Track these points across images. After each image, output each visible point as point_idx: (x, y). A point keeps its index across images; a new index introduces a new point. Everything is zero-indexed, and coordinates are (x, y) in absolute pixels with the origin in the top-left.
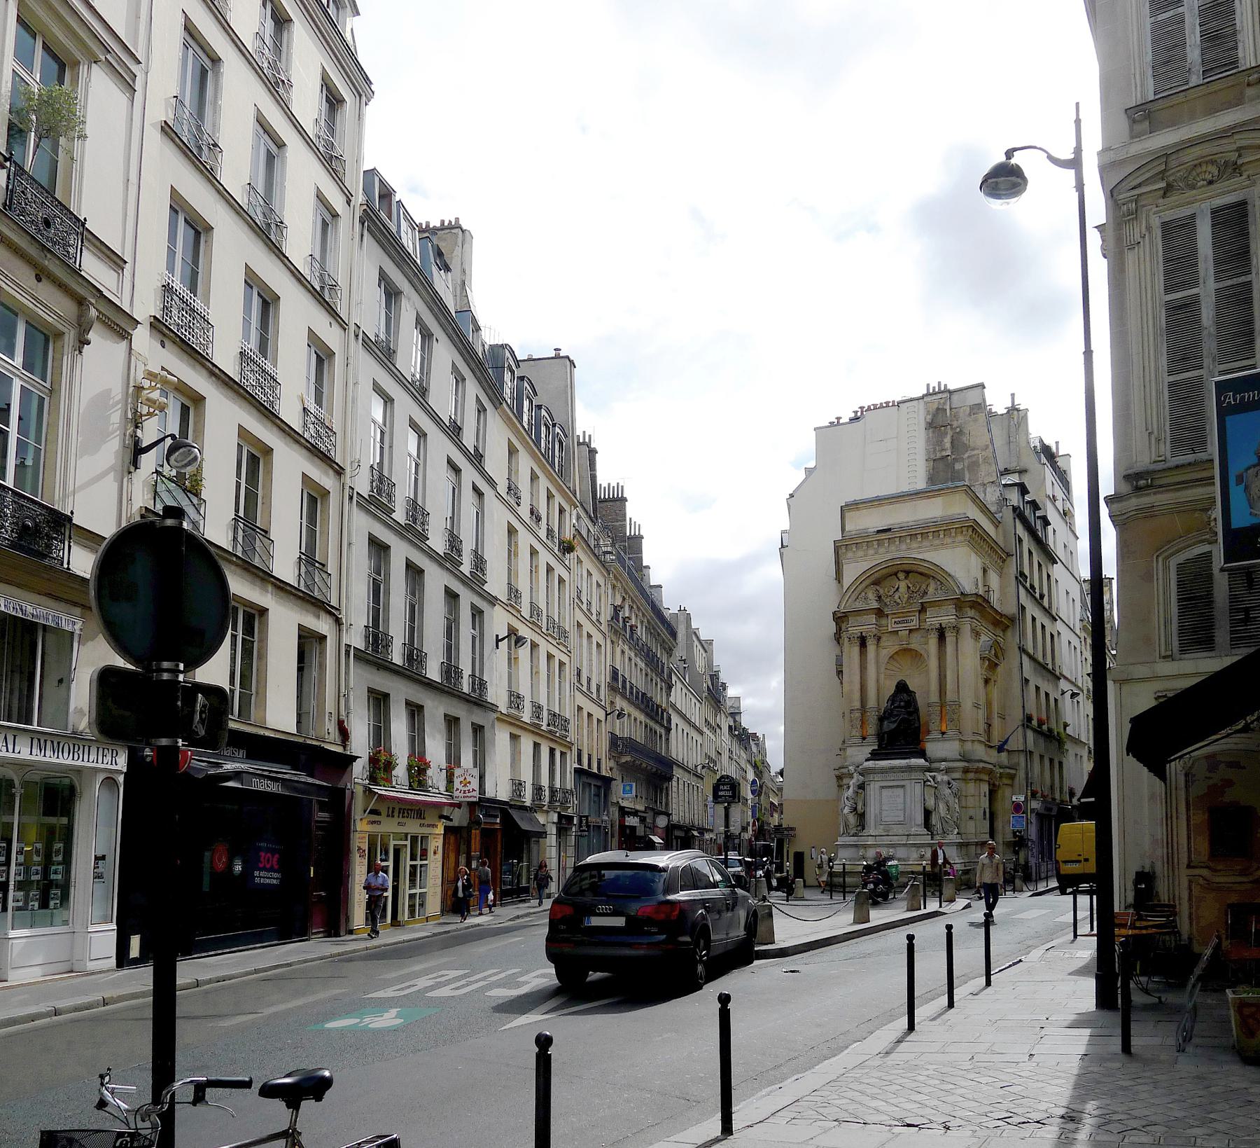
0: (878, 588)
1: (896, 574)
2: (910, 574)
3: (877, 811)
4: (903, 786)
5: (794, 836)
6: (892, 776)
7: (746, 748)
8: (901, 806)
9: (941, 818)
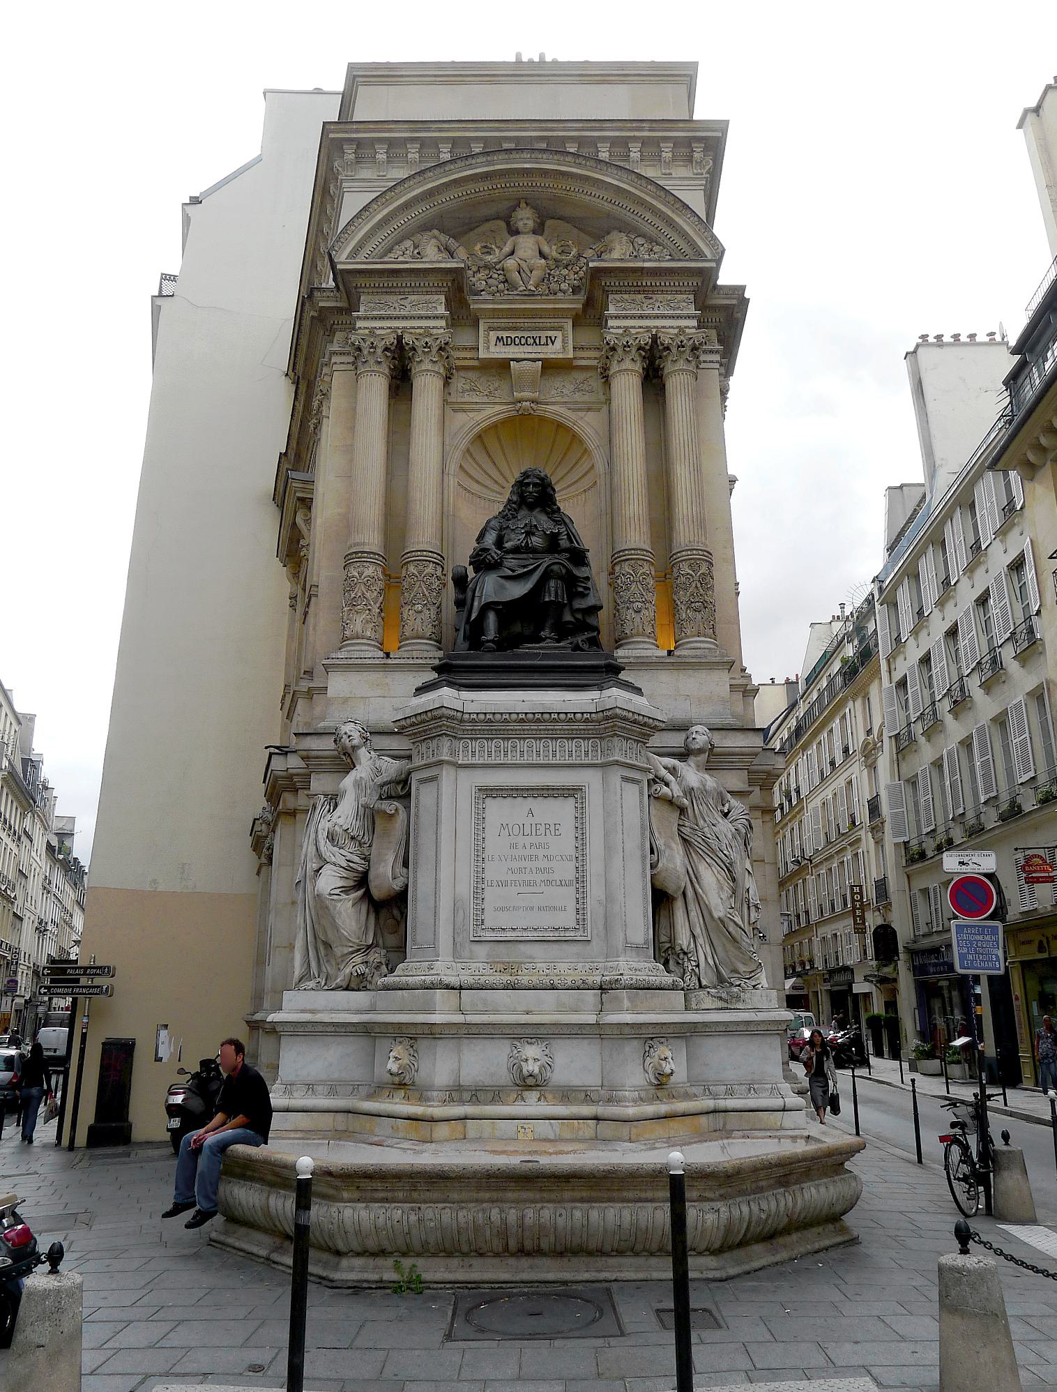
0: (452, 243)
3: (465, 889)
4: (571, 792)
5: (109, 992)
6: (529, 750)
7: (75, 884)
8: (567, 871)
9: (717, 928)
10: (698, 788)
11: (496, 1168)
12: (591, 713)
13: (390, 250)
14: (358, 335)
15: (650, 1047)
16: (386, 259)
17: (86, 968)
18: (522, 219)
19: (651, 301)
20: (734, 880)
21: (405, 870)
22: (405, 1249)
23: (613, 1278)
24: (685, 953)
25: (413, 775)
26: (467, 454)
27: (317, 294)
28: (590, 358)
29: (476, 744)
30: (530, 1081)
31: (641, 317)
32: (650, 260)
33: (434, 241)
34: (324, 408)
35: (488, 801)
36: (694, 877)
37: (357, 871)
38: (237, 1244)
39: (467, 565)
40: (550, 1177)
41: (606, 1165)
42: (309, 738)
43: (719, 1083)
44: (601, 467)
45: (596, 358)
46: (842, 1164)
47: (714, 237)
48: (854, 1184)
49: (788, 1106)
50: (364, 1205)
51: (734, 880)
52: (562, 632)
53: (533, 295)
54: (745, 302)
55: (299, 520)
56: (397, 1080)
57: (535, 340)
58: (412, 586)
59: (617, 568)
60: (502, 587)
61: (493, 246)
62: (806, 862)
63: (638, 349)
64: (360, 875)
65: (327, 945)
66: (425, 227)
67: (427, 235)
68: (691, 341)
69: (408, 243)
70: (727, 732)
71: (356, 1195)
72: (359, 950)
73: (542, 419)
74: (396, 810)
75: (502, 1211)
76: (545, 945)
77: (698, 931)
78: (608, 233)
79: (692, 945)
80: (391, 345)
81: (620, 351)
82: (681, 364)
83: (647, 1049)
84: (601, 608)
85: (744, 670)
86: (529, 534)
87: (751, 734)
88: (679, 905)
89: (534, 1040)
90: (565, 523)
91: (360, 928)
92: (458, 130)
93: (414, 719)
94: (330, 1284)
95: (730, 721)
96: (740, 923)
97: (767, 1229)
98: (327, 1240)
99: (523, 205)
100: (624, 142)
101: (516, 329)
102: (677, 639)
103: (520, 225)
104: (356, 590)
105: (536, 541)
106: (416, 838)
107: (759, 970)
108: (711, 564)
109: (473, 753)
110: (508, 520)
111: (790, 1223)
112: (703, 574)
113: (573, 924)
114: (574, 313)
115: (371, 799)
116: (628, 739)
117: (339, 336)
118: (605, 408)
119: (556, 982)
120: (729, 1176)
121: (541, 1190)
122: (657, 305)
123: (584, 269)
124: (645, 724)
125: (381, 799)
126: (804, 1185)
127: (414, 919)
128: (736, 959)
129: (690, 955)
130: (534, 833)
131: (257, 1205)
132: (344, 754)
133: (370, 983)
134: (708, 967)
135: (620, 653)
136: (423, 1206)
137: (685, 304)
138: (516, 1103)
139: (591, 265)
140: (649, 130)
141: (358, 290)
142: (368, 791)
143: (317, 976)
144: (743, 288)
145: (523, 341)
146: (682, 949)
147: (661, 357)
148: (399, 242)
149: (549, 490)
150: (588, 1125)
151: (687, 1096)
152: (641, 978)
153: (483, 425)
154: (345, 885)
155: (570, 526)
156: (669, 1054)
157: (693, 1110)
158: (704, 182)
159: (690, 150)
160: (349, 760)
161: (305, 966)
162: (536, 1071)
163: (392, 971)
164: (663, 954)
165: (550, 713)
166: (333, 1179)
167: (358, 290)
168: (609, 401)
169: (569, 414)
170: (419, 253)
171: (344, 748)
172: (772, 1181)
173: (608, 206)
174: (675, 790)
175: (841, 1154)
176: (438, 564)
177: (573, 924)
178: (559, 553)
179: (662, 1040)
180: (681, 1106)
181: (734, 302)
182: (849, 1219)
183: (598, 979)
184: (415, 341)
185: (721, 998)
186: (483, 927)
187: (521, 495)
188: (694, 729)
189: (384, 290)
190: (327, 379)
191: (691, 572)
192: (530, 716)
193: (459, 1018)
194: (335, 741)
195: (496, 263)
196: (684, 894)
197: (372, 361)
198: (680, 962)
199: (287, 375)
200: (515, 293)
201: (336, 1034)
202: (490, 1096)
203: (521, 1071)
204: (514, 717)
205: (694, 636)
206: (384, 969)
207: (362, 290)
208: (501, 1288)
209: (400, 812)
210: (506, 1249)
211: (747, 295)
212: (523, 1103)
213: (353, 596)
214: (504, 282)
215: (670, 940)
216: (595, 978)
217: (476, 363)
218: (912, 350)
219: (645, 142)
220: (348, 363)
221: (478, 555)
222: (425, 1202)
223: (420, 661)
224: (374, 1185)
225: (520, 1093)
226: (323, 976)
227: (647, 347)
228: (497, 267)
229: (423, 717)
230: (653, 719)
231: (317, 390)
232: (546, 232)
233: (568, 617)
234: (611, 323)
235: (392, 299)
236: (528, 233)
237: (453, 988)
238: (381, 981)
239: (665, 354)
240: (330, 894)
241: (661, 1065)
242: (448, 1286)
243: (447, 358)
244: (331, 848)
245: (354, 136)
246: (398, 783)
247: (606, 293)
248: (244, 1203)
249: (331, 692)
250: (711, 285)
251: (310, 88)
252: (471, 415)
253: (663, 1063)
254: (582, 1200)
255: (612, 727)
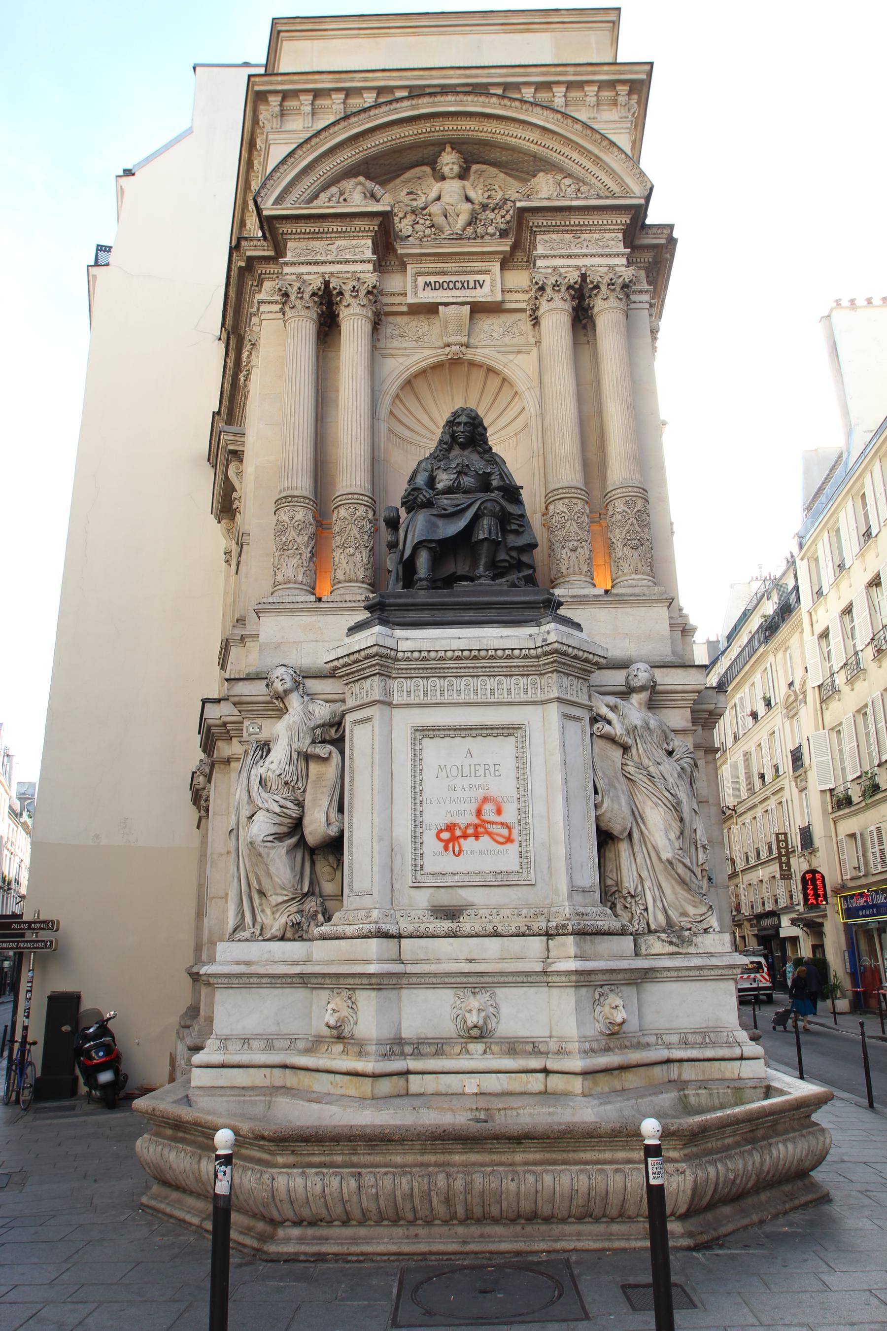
0: (377, 189)
1: (432, 163)
2: (475, 167)
10: (642, 726)
11: (441, 1130)
12: (529, 649)
13: (316, 197)
14: (285, 280)
15: (600, 995)
16: (311, 205)
17: (30, 923)
18: (448, 164)
19: (579, 240)
20: (681, 820)
21: (340, 816)
22: (345, 1218)
23: (572, 1247)
24: (632, 896)
25: (347, 716)
26: (398, 402)
27: (244, 243)
28: (519, 301)
29: (411, 683)
30: (475, 1032)
31: (570, 256)
32: (578, 198)
33: (359, 188)
34: (253, 357)
35: (426, 741)
36: (637, 816)
37: (291, 817)
38: (168, 1210)
39: (399, 506)
40: (501, 1139)
41: (560, 1124)
42: (241, 684)
43: (672, 1031)
44: (532, 407)
45: (524, 301)
46: (809, 1116)
47: (642, 174)
48: (822, 1139)
49: (746, 1054)
50: (300, 1170)
51: (681, 820)
52: (498, 570)
53: (460, 239)
54: (672, 242)
55: (231, 474)
56: (335, 1032)
57: (463, 284)
58: (343, 530)
59: (551, 507)
60: (435, 526)
61: (419, 192)
62: (731, 812)
63: (568, 288)
64: (294, 822)
65: (262, 893)
66: (350, 173)
67: (353, 181)
68: (621, 279)
69: (334, 190)
70: (669, 669)
71: (292, 1159)
72: (293, 899)
73: (472, 364)
74: (330, 754)
75: (448, 1175)
76: (487, 889)
77: (644, 874)
78: (535, 176)
79: (640, 888)
80: (319, 289)
81: (549, 290)
82: (612, 302)
83: (597, 996)
84: (536, 546)
85: (680, 610)
86: (459, 473)
87: (693, 671)
88: (624, 847)
89: (477, 990)
90: (496, 462)
91: (295, 876)
92: (384, 79)
93: (346, 659)
94: (265, 1257)
95: (670, 658)
96: (689, 864)
97: (734, 1190)
98: (262, 1209)
99: (448, 149)
100: (547, 86)
101: (443, 273)
102: (614, 576)
103: (446, 170)
104: (287, 534)
105: (468, 481)
106: (352, 780)
107: (710, 913)
108: (647, 501)
109: (409, 693)
110: (440, 461)
111: (757, 1182)
112: (639, 511)
113: (517, 868)
114: (501, 256)
115: (305, 744)
116: (569, 675)
117: (267, 285)
118: (535, 349)
119: (500, 929)
120: (694, 1135)
121: (490, 1152)
122: (585, 244)
123: (511, 212)
124: (586, 661)
125: (313, 742)
126: (773, 1140)
127: (351, 865)
128: (685, 901)
129: (637, 899)
130: (473, 774)
131: (188, 1169)
132: (277, 698)
133: (307, 932)
134: (657, 909)
135: (557, 592)
136: (363, 1171)
137: (613, 243)
138: (461, 1056)
139: (519, 205)
140: (574, 75)
141: (285, 237)
142: (301, 735)
143: (251, 926)
144: (671, 227)
145: (451, 285)
146: (629, 893)
147: (590, 297)
148: (324, 188)
149: (480, 429)
150: (537, 1079)
151: (639, 1046)
152: (589, 923)
153: (413, 370)
154: (278, 831)
155: (503, 467)
156: (619, 1002)
157: (648, 1061)
158: (629, 125)
159: (614, 93)
160: (282, 705)
161: (240, 916)
162: (481, 1022)
163: (328, 919)
164: (610, 898)
165: (487, 650)
166: (266, 1143)
167: (285, 237)
168: (538, 343)
169: (499, 356)
170: (345, 200)
171: (276, 692)
172: (738, 1138)
173: (533, 147)
174: (617, 729)
175: (808, 1106)
176: (370, 507)
177: (517, 868)
178: (492, 491)
179: (613, 987)
180: (635, 1056)
181: (663, 241)
182: (817, 1175)
183: (543, 925)
184: (342, 285)
185: (671, 943)
186: (422, 872)
187: (453, 436)
188: (635, 666)
189: (311, 236)
190: (256, 329)
191: (626, 509)
192: (466, 653)
193: (397, 968)
194: (267, 685)
195: (424, 209)
196: (630, 836)
197: (299, 307)
198: (628, 905)
199: (220, 339)
200: (443, 236)
201: (272, 986)
202: (433, 1049)
203: (465, 1022)
204: (449, 654)
205: (631, 574)
206: (320, 917)
207: (289, 237)
208: (450, 1259)
209: (334, 755)
210: (454, 1216)
211: (675, 235)
212: (468, 1056)
213: (284, 540)
214: (430, 227)
215: (617, 882)
216: (540, 924)
217: (405, 309)
218: (826, 314)
219: (570, 85)
220: (276, 312)
221: (409, 494)
222: (365, 1166)
223: (353, 605)
224: (311, 1148)
225: (464, 1045)
226: (258, 927)
227: (577, 286)
228: (424, 212)
229: (356, 656)
230: (594, 655)
231: (246, 339)
232: (472, 178)
233: (502, 556)
234: (539, 263)
235: (318, 245)
236: (453, 178)
237: (392, 937)
238: (317, 931)
239: (595, 292)
240: (264, 841)
241: (612, 1014)
242: (392, 1258)
243: (375, 302)
244: (264, 795)
245: (279, 88)
246: (332, 726)
247: (534, 234)
248: (175, 1166)
249: (262, 638)
250: (640, 224)
251: (240, 62)
252: (401, 360)
253: (613, 1011)
254: (535, 1163)
255: (552, 662)
